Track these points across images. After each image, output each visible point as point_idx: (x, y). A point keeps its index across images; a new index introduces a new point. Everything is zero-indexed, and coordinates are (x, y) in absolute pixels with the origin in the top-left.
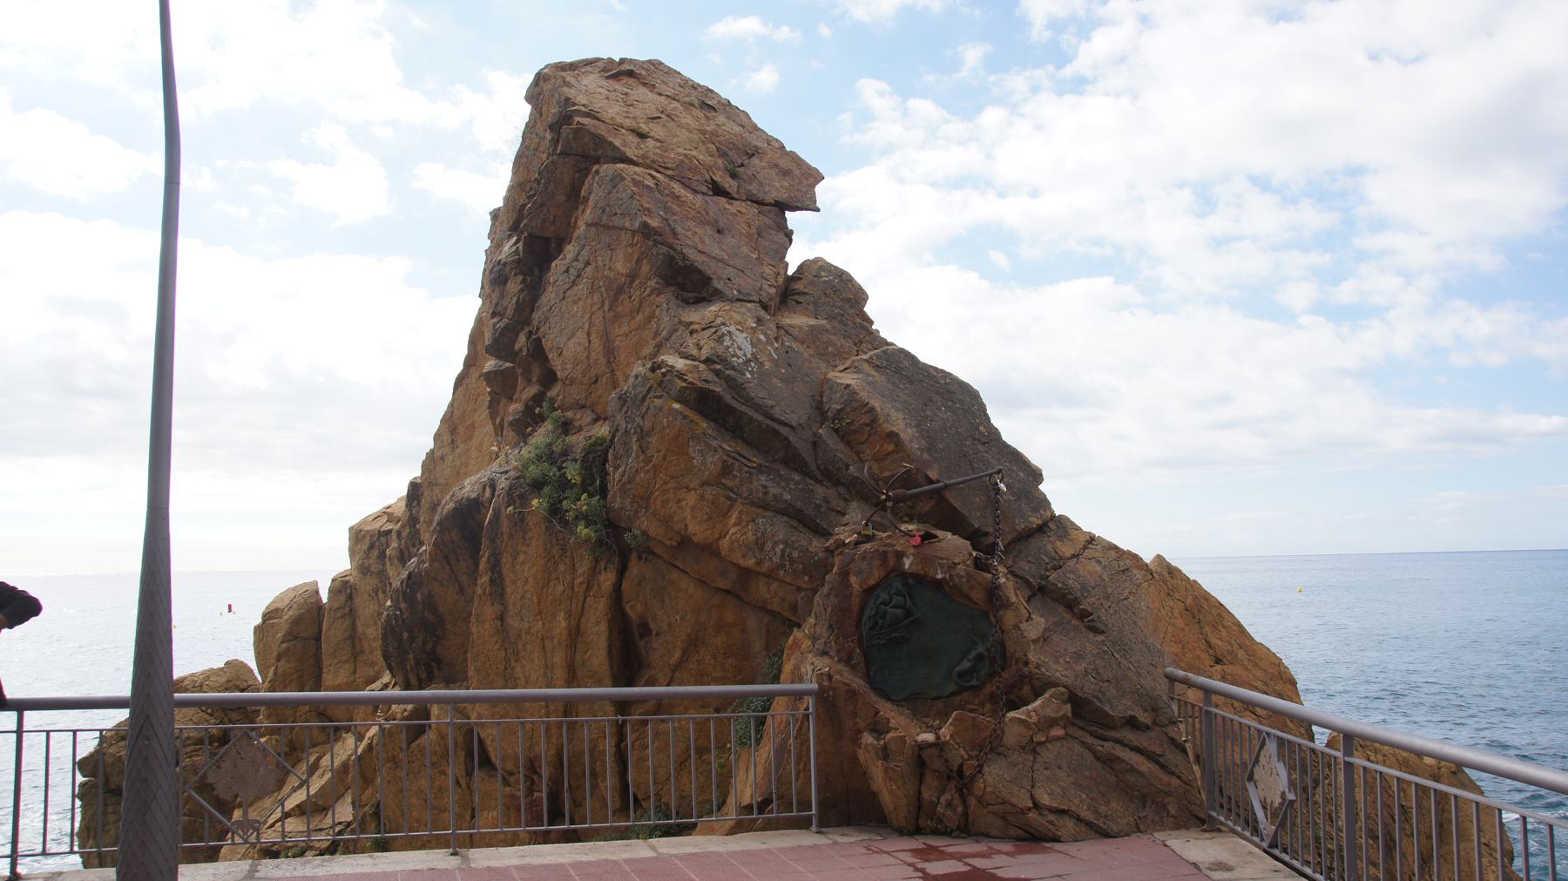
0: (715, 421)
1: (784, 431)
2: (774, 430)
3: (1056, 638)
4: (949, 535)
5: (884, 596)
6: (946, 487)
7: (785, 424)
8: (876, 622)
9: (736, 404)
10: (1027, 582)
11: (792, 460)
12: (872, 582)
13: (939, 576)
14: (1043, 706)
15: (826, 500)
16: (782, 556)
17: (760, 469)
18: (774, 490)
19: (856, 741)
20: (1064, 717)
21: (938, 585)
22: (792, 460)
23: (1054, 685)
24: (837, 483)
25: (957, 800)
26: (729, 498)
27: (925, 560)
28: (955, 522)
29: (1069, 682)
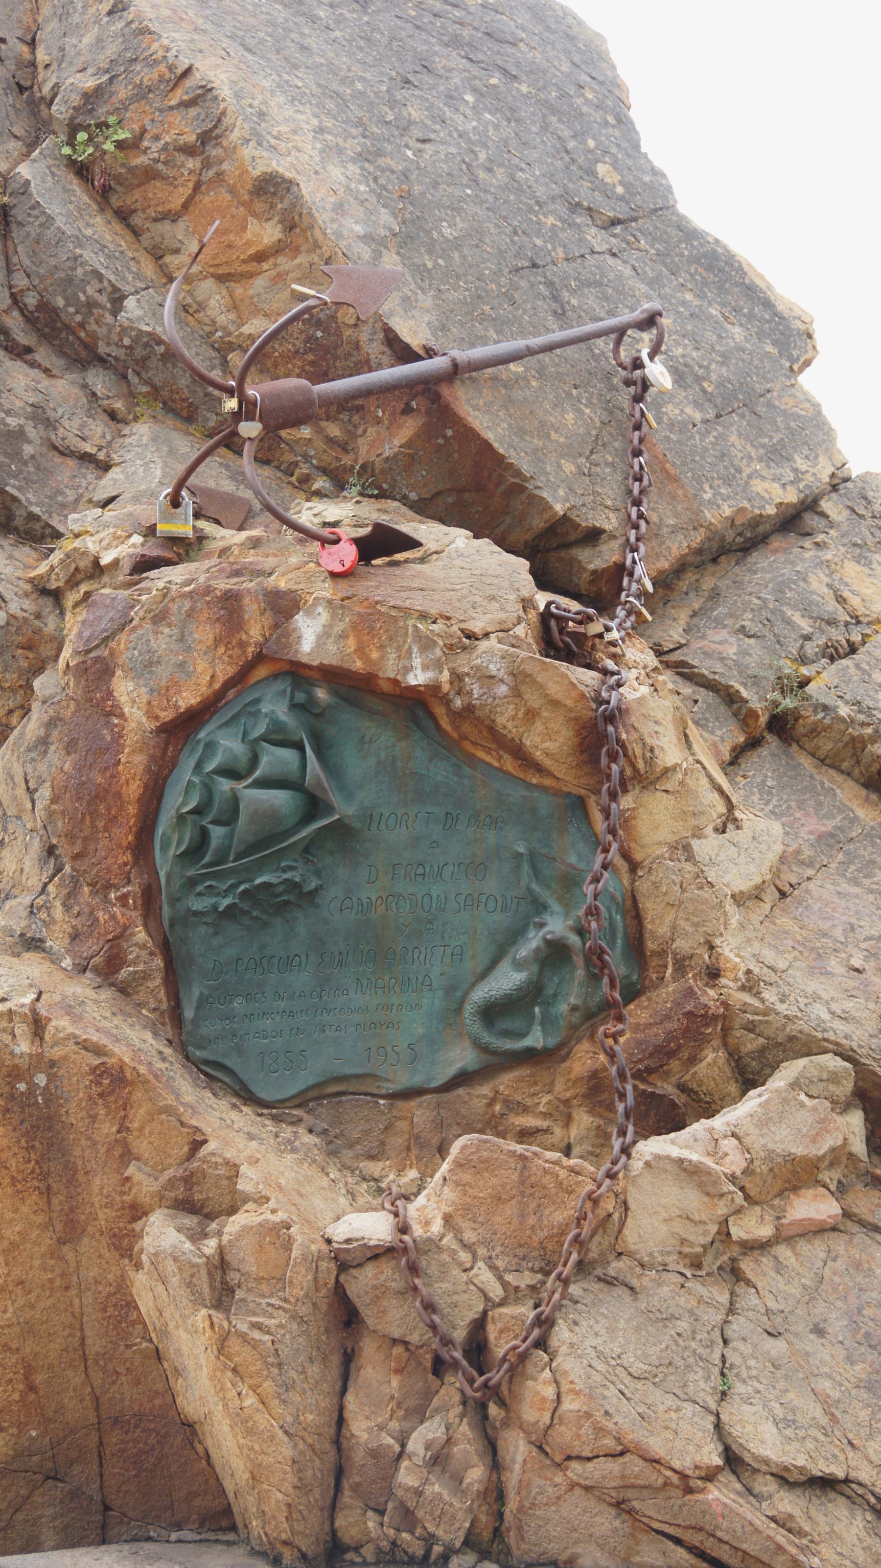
12: (188, 698)
13: (417, 678)
21: (414, 707)
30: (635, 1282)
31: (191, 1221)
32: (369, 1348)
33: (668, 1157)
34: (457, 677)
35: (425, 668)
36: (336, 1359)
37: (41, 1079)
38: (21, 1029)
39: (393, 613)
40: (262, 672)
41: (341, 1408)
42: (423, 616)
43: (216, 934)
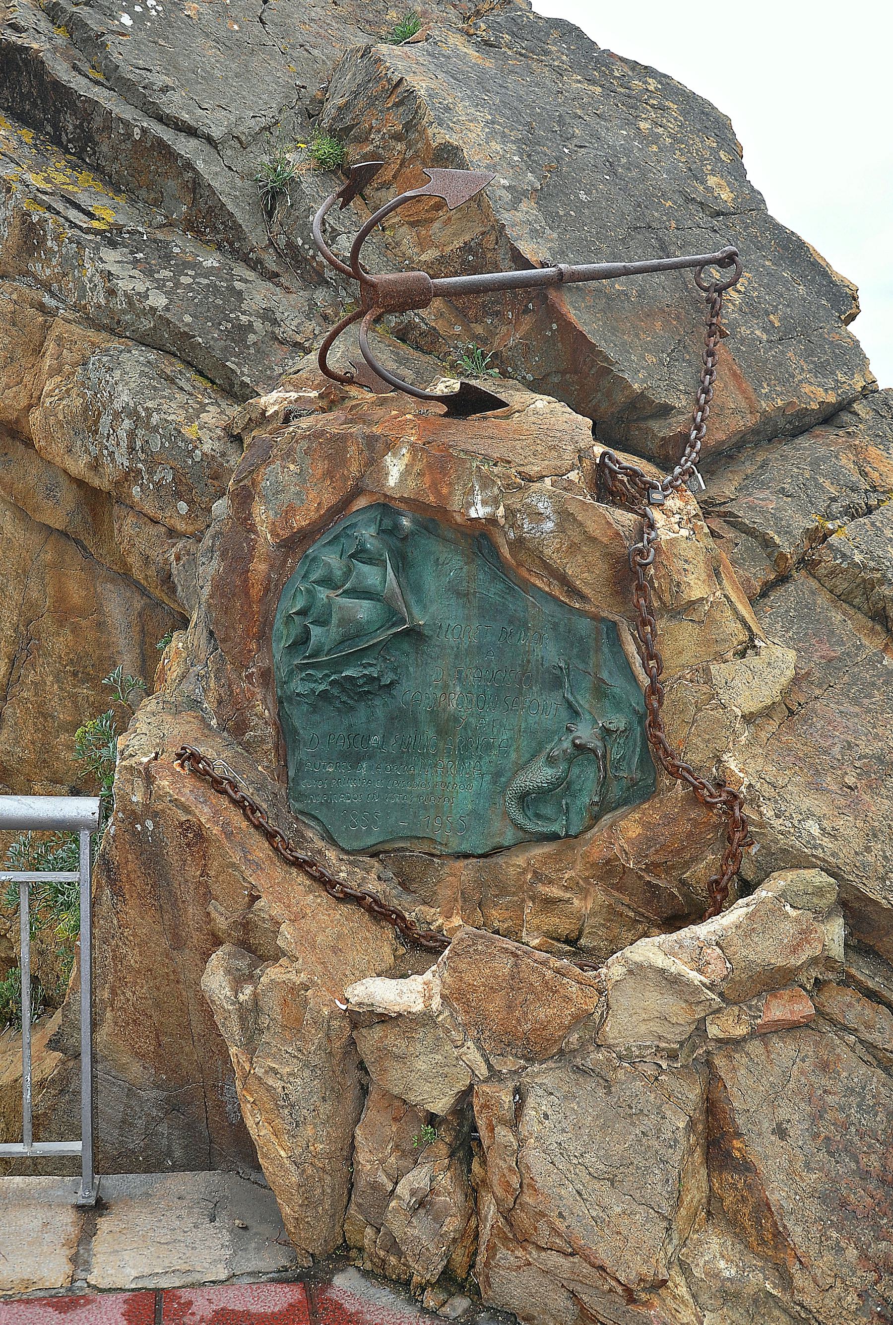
0: (36, 126)
1: (185, 147)
2: (161, 145)
3: (828, 707)
4: (541, 402)
6: (561, 280)
7: (191, 132)
8: (304, 639)
9: (79, 84)
10: (767, 543)
11: (208, 221)
12: (300, 522)
13: (479, 511)
14: (747, 930)
15: (268, 316)
16: (131, 449)
17: (112, 237)
18: (130, 282)
21: (479, 539)
22: (208, 221)
23: (799, 862)
25: (450, 1197)
26: (42, 308)
27: (439, 463)
29: (844, 854)
30: (611, 1075)
31: (242, 964)
32: (374, 1095)
33: (650, 966)
34: (511, 513)
35: (484, 503)
36: (351, 1094)
37: (149, 824)
38: (139, 783)
39: (462, 455)
40: (361, 502)
41: (353, 1137)
42: (486, 458)
43: (314, 712)
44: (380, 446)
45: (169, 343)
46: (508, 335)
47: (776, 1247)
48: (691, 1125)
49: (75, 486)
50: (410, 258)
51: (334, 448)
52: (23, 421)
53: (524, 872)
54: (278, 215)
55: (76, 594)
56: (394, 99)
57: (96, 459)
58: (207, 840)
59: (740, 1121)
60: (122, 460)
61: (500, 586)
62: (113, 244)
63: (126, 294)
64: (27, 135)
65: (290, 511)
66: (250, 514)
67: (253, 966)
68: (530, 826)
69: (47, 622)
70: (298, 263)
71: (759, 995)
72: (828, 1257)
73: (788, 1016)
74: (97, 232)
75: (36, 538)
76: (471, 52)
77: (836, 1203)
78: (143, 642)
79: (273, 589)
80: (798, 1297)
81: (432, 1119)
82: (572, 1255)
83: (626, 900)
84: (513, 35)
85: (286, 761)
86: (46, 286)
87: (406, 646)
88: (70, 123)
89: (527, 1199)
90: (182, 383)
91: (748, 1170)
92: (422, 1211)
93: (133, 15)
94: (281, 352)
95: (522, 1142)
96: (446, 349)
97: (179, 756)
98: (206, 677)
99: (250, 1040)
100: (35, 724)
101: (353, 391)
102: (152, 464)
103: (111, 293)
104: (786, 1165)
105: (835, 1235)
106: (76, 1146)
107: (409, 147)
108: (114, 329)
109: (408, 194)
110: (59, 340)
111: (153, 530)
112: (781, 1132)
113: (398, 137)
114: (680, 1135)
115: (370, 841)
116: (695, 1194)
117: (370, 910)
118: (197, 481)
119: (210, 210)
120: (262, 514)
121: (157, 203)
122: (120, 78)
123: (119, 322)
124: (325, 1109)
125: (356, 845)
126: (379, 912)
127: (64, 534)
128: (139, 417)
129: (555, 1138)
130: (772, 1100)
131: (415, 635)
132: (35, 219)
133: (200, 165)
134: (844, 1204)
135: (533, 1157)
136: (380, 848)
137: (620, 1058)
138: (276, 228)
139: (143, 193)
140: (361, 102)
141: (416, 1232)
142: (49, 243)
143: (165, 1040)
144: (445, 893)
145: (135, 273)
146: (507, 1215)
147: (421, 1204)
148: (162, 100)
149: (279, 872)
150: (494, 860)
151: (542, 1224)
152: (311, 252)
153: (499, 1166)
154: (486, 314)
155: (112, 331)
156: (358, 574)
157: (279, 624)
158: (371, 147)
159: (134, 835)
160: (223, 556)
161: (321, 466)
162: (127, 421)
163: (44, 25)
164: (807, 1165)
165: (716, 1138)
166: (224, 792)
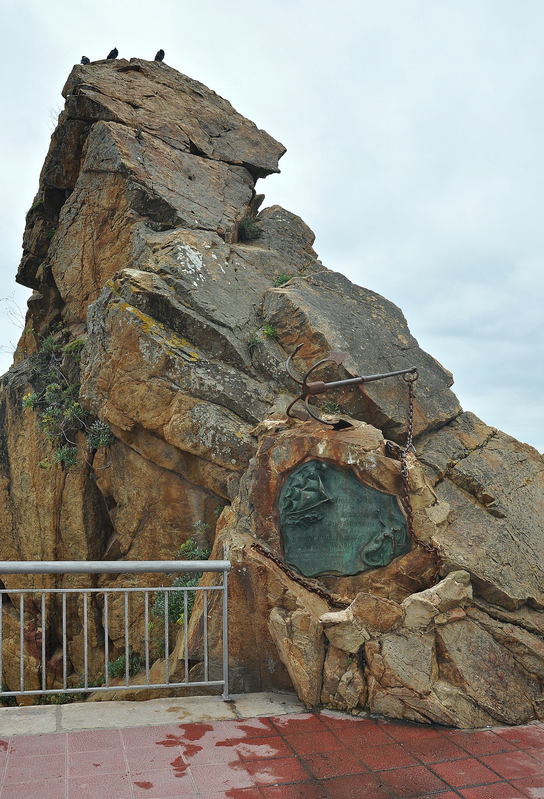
0: (164, 322)
1: (223, 331)
3: (460, 522)
4: (363, 424)
5: (300, 479)
7: (224, 326)
8: (291, 504)
9: (181, 308)
10: (435, 469)
11: (229, 356)
12: (288, 466)
13: (351, 462)
14: (445, 589)
15: (256, 392)
16: (213, 440)
17: (198, 364)
18: (209, 381)
19: (266, 615)
20: (466, 599)
21: (349, 470)
22: (229, 356)
24: (269, 377)
25: (359, 680)
26: (171, 389)
27: (337, 446)
28: (371, 414)
29: (471, 564)
30: (407, 636)
31: (283, 612)
32: (331, 650)
33: (418, 601)
34: (361, 462)
35: (353, 459)
36: (323, 652)
37: (244, 569)
38: (240, 555)
39: (344, 444)
40: (308, 459)
41: (324, 666)
42: (352, 445)
43: (294, 530)
44: (315, 441)
45: (226, 404)
46: (343, 399)
47: (461, 682)
48: (433, 649)
49: (180, 453)
50: (304, 371)
51: (300, 442)
52: (160, 429)
53: (369, 579)
54: (255, 354)
55: (175, 493)
56: (295, 314)
57: (196, 444)
58: (268, 572)
59: (447, 647)
60: (209, 444)
61: (357, 486)
62: (199, 367)
63: (208, 385)
64: (161, 325)
65: (284, 463)
66: (268, 464)
67: (287, 613)
68: (370, 564)
69: (160, 505)
70: (263, 372)
71: (449, 610)
72: (476, 682)
73: (458, 616)
74: (193, 362)
75: (157, 473)
76: (310, 289)
77: (477, 668)
78: (205, 511)
79: (279, 489)
80: (468, 694)
81: (351, 655)
82: (403, 687)
83: (403, 586)
84: (323, 280)
85: (284, 548)
86: (173, 381)
87: (325, 506)
88: (177, 322)
89: (387, 672)
90: (231, 417)
91: (451, 661)
92: (350, 685)
93: (196, 281)
94: (262, 405)
95: (383, 657)
96: (320, 403)
97: (252, 546)
98: (250, 520)
99: (290, 635)
100: (149, 546)
101: (297, 421)
102: (222, 445)
103: (202, 385)
104: (461, 658)
105: (477, 676)
106: (223, 682)
107: (302, 331)
108: (202, 397)
109: (324, 360)
110: (180, 401)
111: (219, 470)
112: (459, 650)
113: (297, 328)
114: (430, 652)
115: (315, 573)
116: (435, 671)
117: (319, 594)
118: (241, 453)
119: (231, 353)
120: (273, 464)
121: (210, 350)
122: (198, 306)
123: (204, 395)
124: (316, 656)
125: (310, 574)
126: (323, 596)
127: (172, 471)
128: (217, 429)
129: (394, 654)
130: (456, 641)
131: (330, 503)
132: (171, 358)
133: (228, 338)
134: (479, 668)
135: (388, 660)
136: (318, 575)
137: (410, 631)
138: (254, 359)
139: (204, 346)
140: (282, 314)
141: (349, 691)
142: (176, 366)
143: (244, 647)
144: (341, 589)
145: (209, 377)
146: (379, 680)
147: (350, 683)
148: (213, 314)
149: (291, 582)
150: (358, 576)
151: (393, 680)
152: (268, 368)
153: (376, 667)
154: (334, 391)
155: (201, 398)
156: (310, 483)
157: (281, 501)
158: (286, 330)
159: (237, 574)
160: (257, 478)
161: (295, 448)
162: (212, 431)
163: (166, 286)
164: (468, 659)
165: (440, 653)
166: (269, 557)
